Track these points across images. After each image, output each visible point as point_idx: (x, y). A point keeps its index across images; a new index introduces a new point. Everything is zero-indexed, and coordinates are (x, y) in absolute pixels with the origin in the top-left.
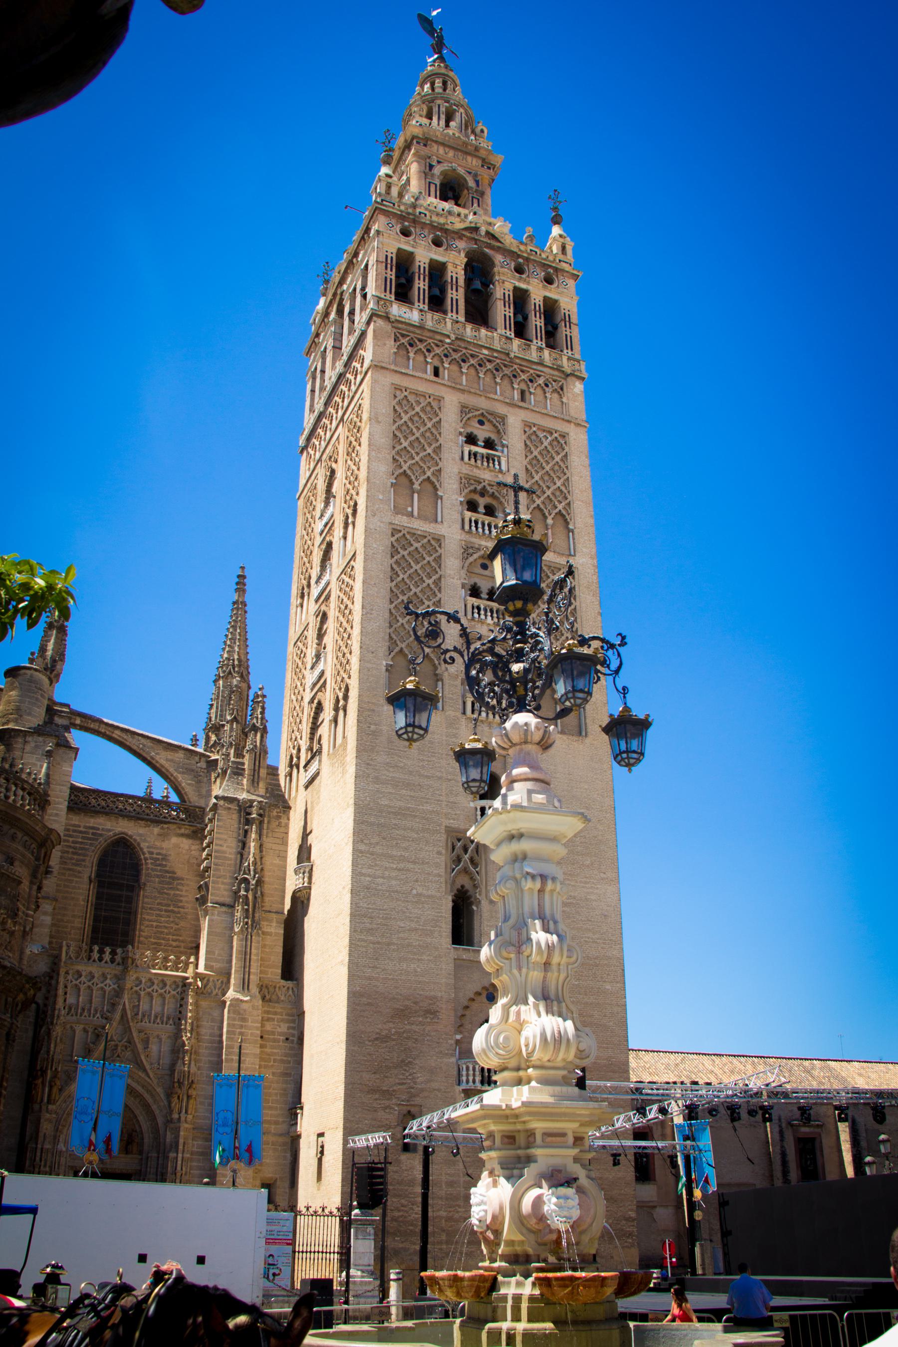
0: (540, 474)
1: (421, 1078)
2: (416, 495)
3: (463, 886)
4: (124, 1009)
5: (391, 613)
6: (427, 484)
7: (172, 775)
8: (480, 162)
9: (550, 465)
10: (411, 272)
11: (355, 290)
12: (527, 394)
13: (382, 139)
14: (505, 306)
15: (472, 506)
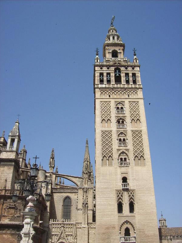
1: (112, 241)
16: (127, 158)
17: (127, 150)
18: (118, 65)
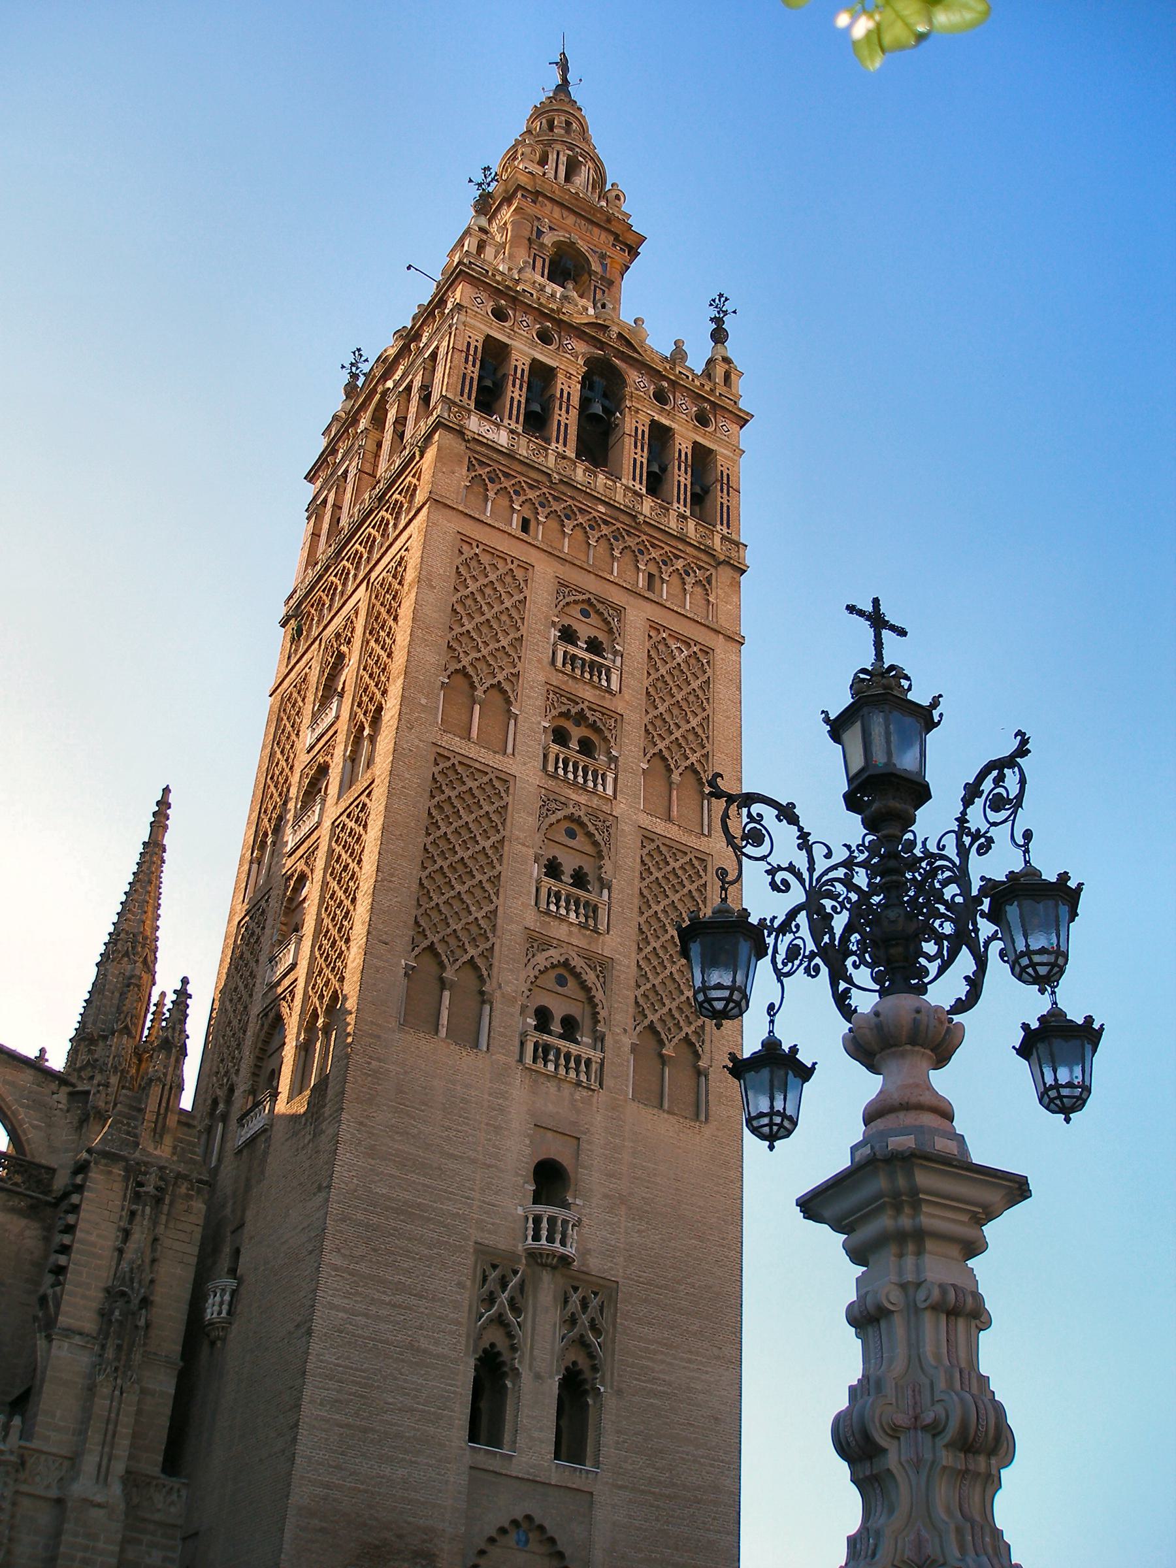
0: (666, 704)
2: (477, 707)
3: (492, 1345)
5: (421, 884)
6: (494, 693)
7: (10, 1108)
9: (683, 693)
10: (499, 375)
11: (409, 388)
12: (657, 580)
13: (479, 178)
14: (636, 447)
15: (560, 736)
16: (586, 1024)
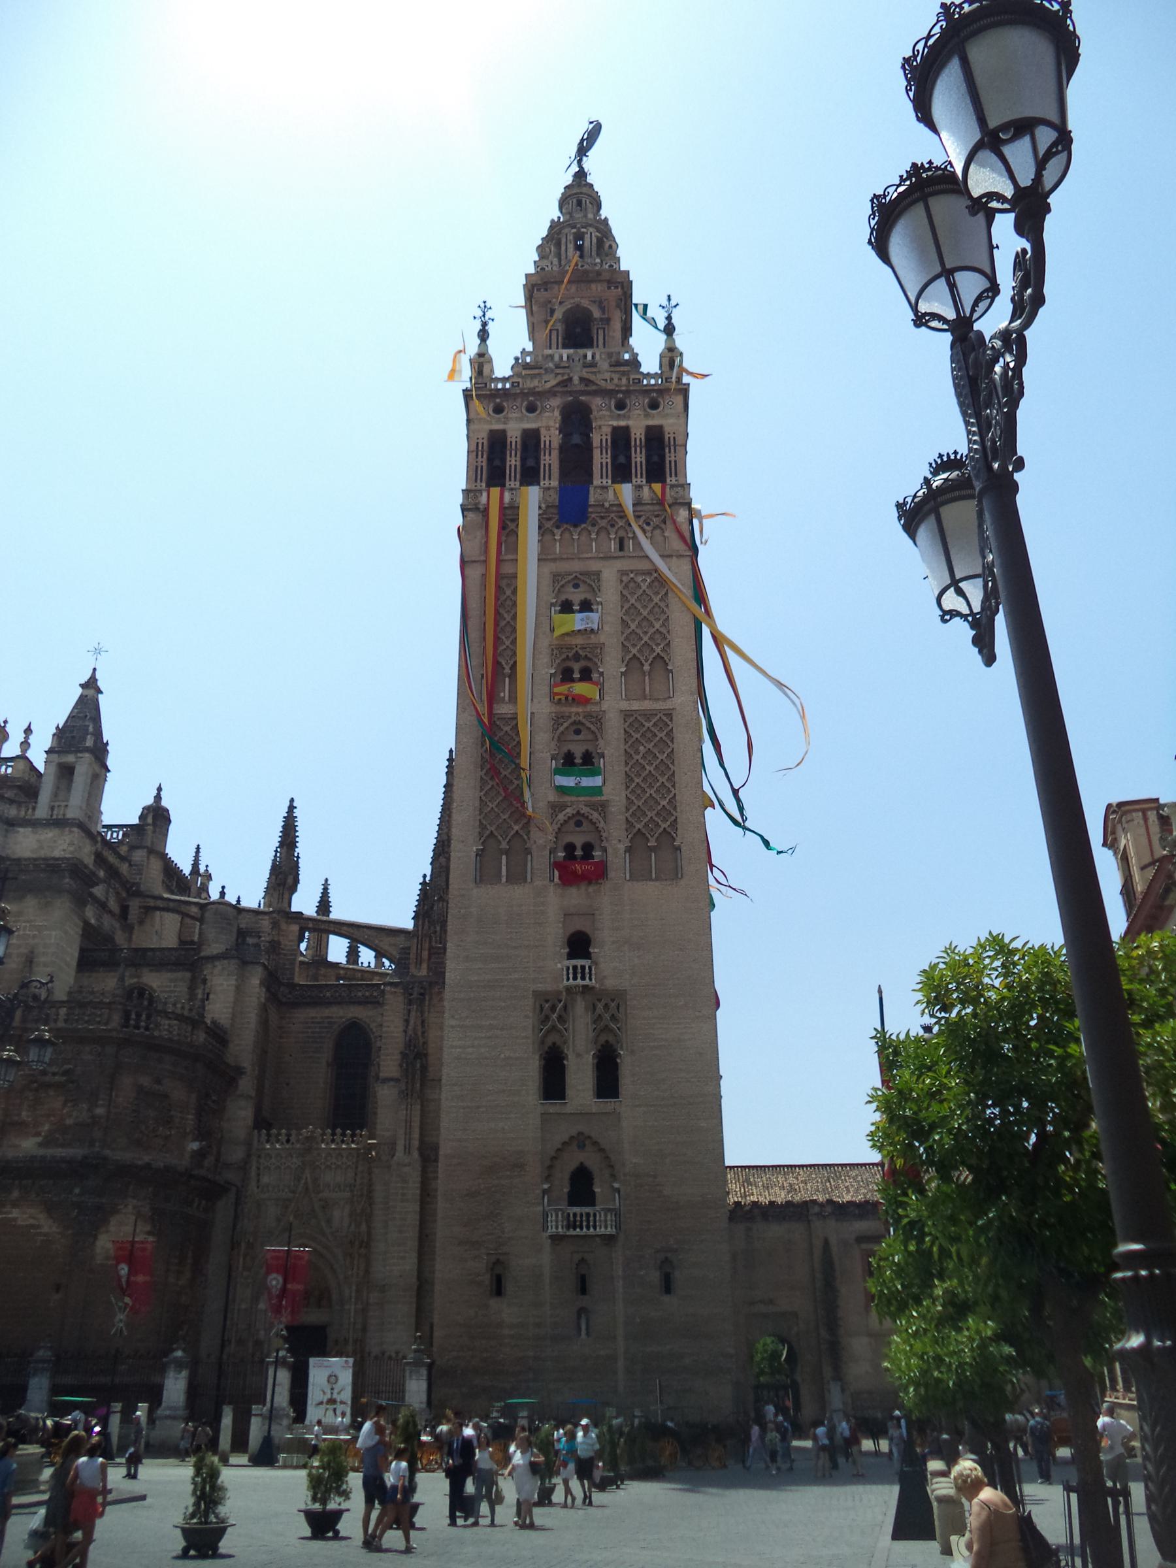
2: (507, 680)
4: (306, 1183)
8: (605, 285)
17: (592, 806)
18: (582, 387)
